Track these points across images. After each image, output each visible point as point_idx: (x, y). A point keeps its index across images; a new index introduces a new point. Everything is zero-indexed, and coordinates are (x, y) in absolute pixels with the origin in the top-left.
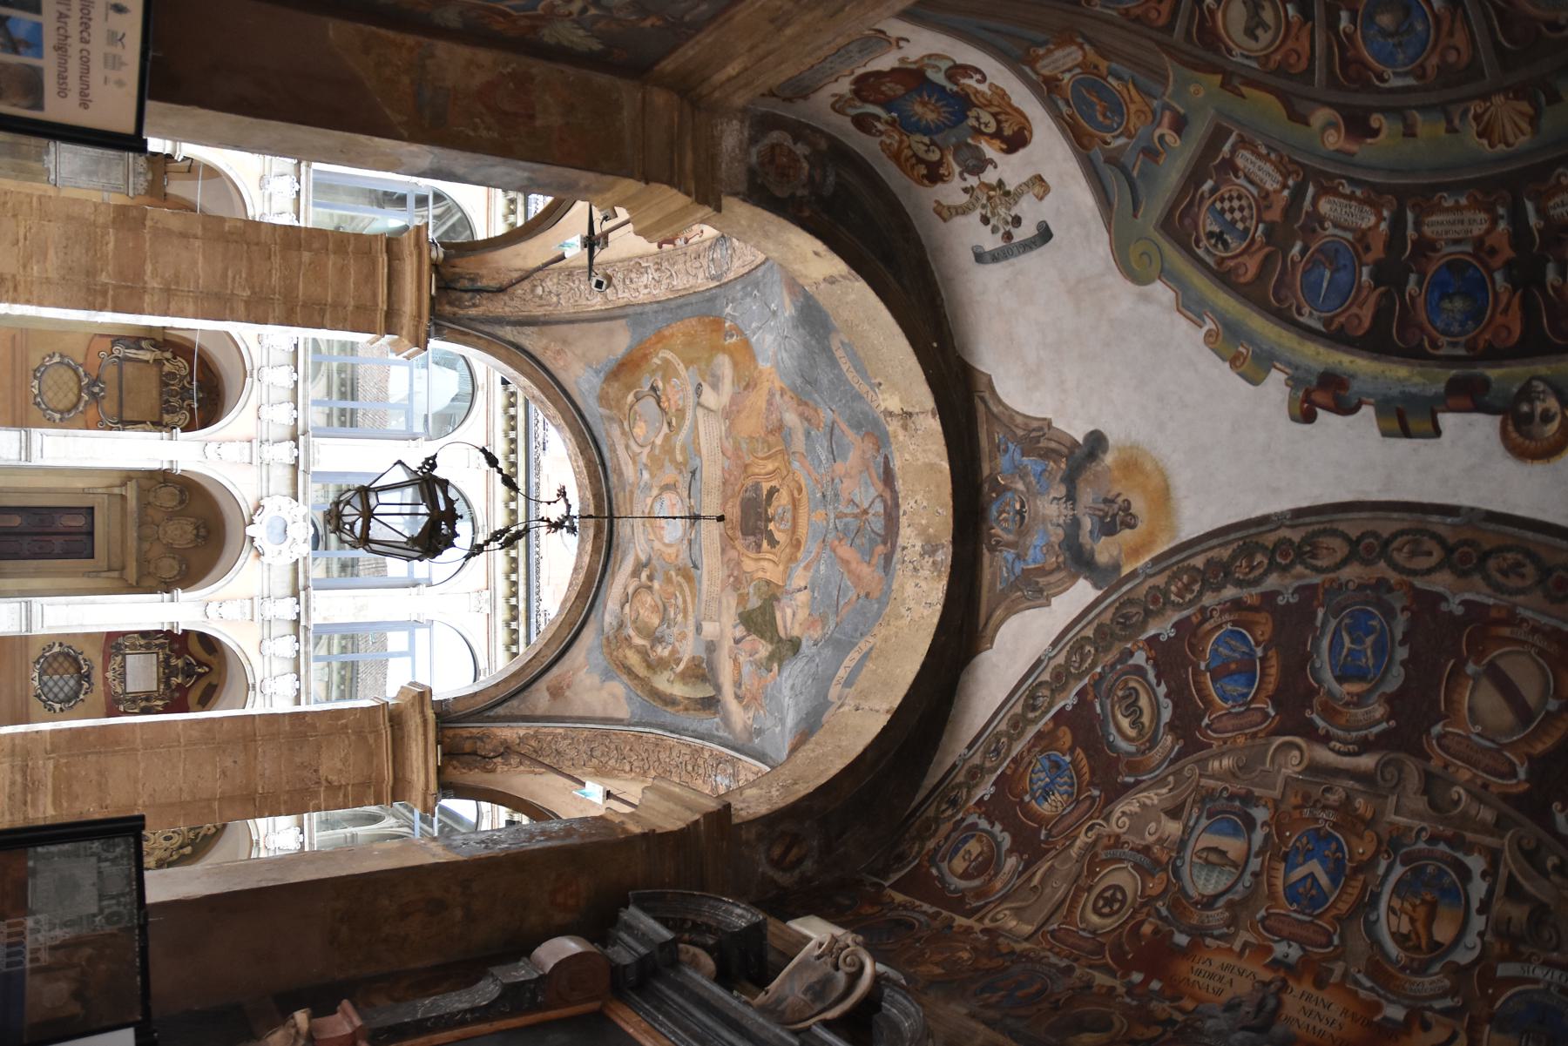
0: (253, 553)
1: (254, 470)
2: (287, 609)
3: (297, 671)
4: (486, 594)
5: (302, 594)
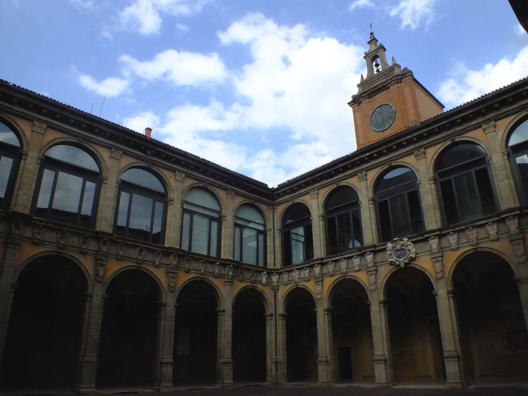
0: (413, 262)
1: (379, 269)
2: (434, 243)
4: (416, 152)
5: (426, 236)
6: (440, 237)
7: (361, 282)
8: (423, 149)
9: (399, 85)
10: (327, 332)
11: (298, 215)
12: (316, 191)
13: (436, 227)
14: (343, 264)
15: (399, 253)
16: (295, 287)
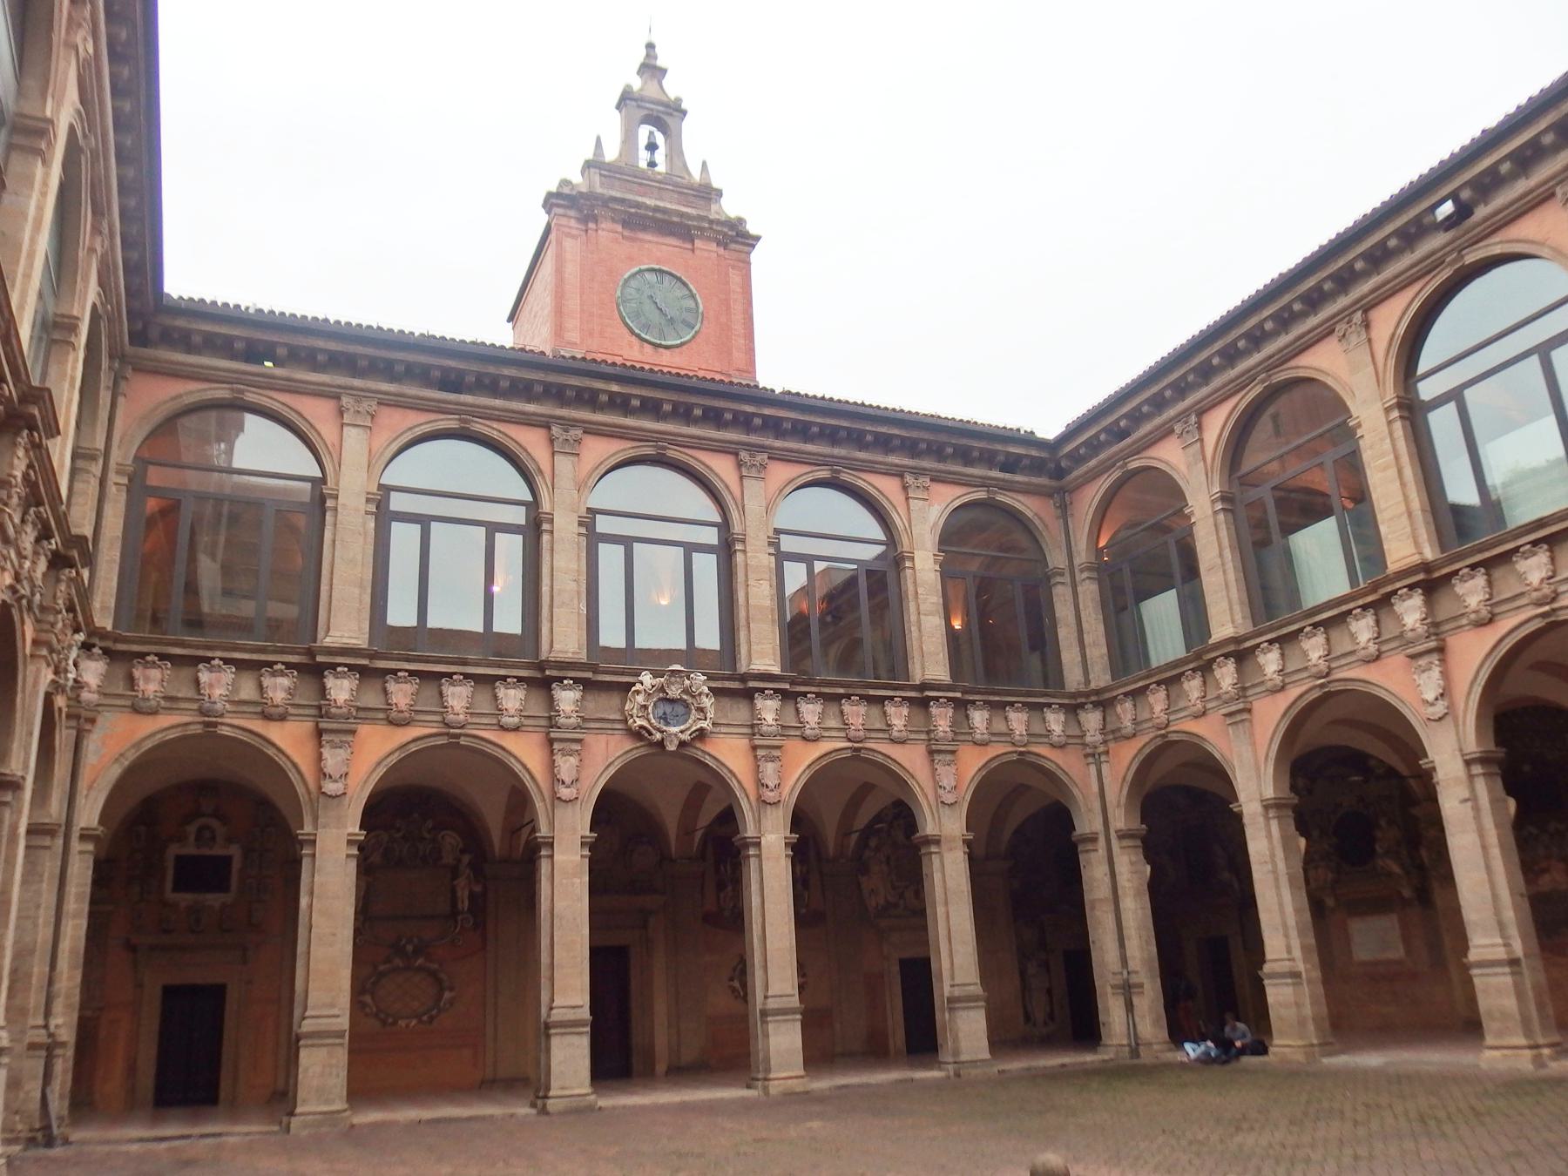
3: (837, 698)
5: (751, 684)
7: (517, 768)
8: (765, 456)
9: (721, 251)
12: (365, 406)
14: (458, 697)
15: (668, 708)
16: (198, 729)
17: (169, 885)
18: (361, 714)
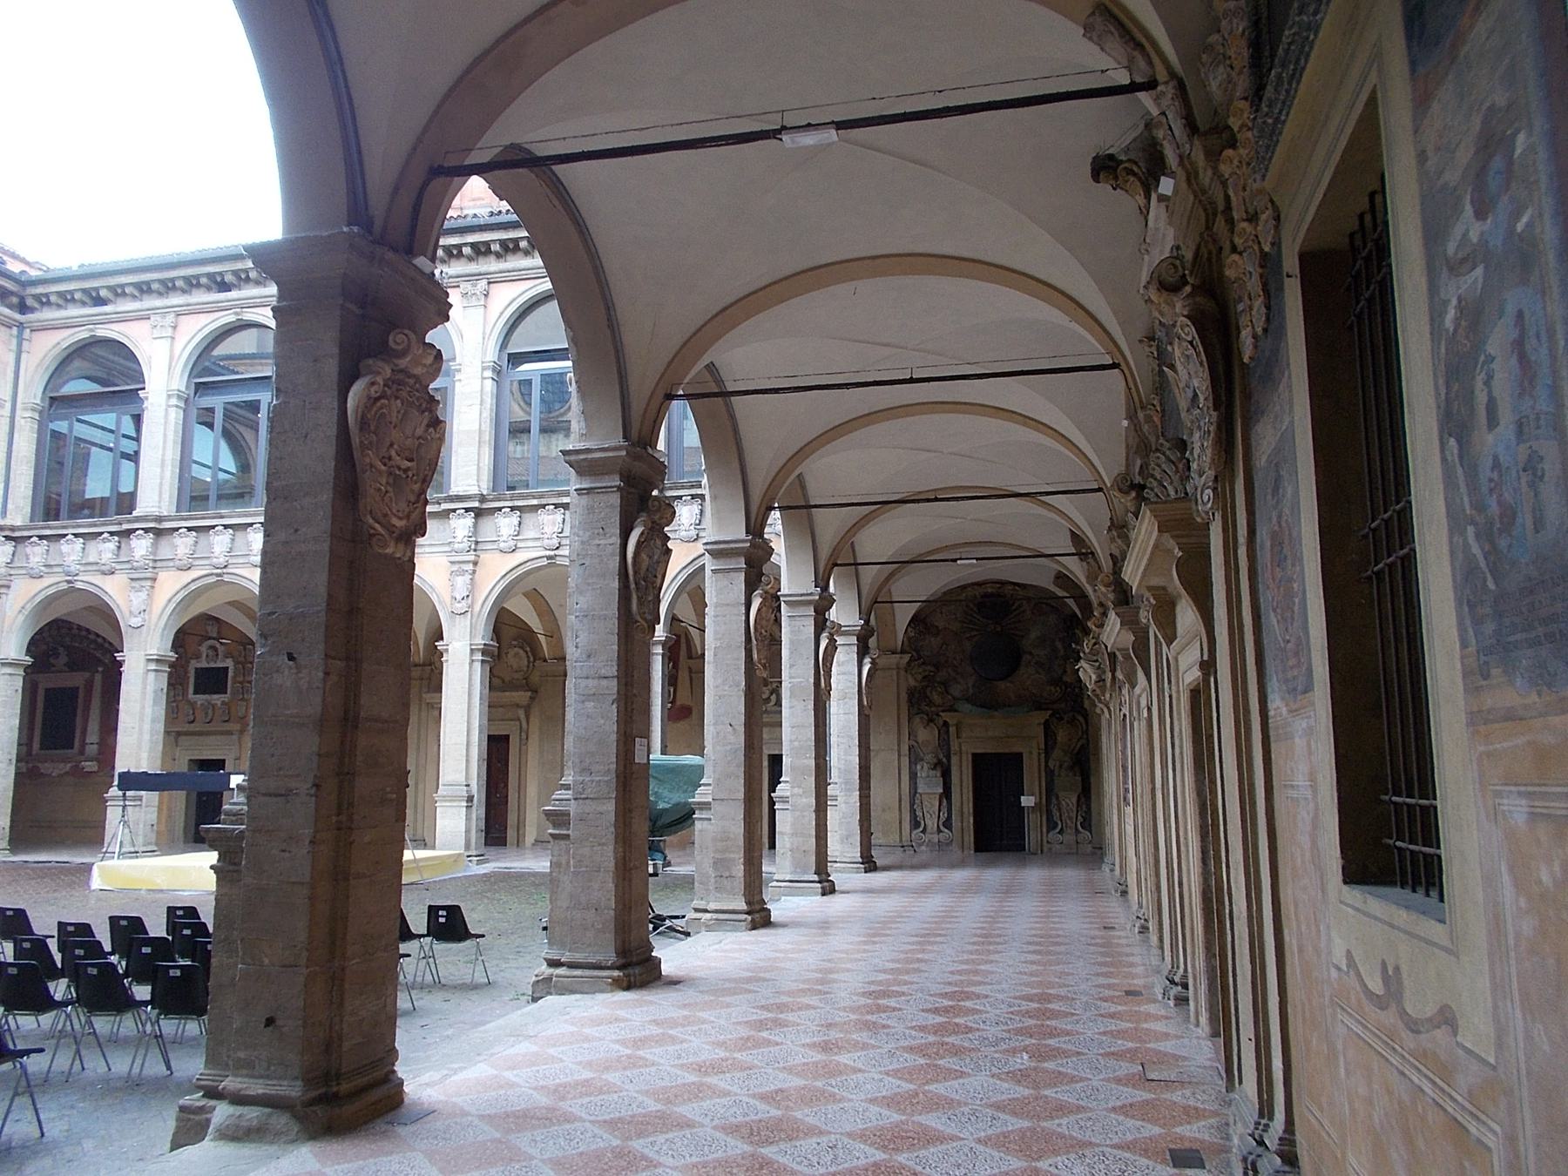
3: (535, 508)
6: (479, 513)
8: (485, 282)
10: (148, 720)
11: (107, 374)
12: (170, 318)
13: (474, 490)
16: (65, 586)
17: (191, 690)
18: (159, 564)
